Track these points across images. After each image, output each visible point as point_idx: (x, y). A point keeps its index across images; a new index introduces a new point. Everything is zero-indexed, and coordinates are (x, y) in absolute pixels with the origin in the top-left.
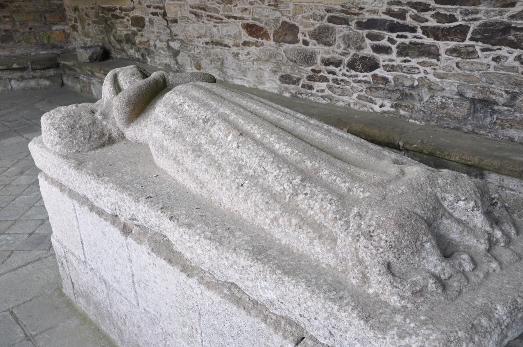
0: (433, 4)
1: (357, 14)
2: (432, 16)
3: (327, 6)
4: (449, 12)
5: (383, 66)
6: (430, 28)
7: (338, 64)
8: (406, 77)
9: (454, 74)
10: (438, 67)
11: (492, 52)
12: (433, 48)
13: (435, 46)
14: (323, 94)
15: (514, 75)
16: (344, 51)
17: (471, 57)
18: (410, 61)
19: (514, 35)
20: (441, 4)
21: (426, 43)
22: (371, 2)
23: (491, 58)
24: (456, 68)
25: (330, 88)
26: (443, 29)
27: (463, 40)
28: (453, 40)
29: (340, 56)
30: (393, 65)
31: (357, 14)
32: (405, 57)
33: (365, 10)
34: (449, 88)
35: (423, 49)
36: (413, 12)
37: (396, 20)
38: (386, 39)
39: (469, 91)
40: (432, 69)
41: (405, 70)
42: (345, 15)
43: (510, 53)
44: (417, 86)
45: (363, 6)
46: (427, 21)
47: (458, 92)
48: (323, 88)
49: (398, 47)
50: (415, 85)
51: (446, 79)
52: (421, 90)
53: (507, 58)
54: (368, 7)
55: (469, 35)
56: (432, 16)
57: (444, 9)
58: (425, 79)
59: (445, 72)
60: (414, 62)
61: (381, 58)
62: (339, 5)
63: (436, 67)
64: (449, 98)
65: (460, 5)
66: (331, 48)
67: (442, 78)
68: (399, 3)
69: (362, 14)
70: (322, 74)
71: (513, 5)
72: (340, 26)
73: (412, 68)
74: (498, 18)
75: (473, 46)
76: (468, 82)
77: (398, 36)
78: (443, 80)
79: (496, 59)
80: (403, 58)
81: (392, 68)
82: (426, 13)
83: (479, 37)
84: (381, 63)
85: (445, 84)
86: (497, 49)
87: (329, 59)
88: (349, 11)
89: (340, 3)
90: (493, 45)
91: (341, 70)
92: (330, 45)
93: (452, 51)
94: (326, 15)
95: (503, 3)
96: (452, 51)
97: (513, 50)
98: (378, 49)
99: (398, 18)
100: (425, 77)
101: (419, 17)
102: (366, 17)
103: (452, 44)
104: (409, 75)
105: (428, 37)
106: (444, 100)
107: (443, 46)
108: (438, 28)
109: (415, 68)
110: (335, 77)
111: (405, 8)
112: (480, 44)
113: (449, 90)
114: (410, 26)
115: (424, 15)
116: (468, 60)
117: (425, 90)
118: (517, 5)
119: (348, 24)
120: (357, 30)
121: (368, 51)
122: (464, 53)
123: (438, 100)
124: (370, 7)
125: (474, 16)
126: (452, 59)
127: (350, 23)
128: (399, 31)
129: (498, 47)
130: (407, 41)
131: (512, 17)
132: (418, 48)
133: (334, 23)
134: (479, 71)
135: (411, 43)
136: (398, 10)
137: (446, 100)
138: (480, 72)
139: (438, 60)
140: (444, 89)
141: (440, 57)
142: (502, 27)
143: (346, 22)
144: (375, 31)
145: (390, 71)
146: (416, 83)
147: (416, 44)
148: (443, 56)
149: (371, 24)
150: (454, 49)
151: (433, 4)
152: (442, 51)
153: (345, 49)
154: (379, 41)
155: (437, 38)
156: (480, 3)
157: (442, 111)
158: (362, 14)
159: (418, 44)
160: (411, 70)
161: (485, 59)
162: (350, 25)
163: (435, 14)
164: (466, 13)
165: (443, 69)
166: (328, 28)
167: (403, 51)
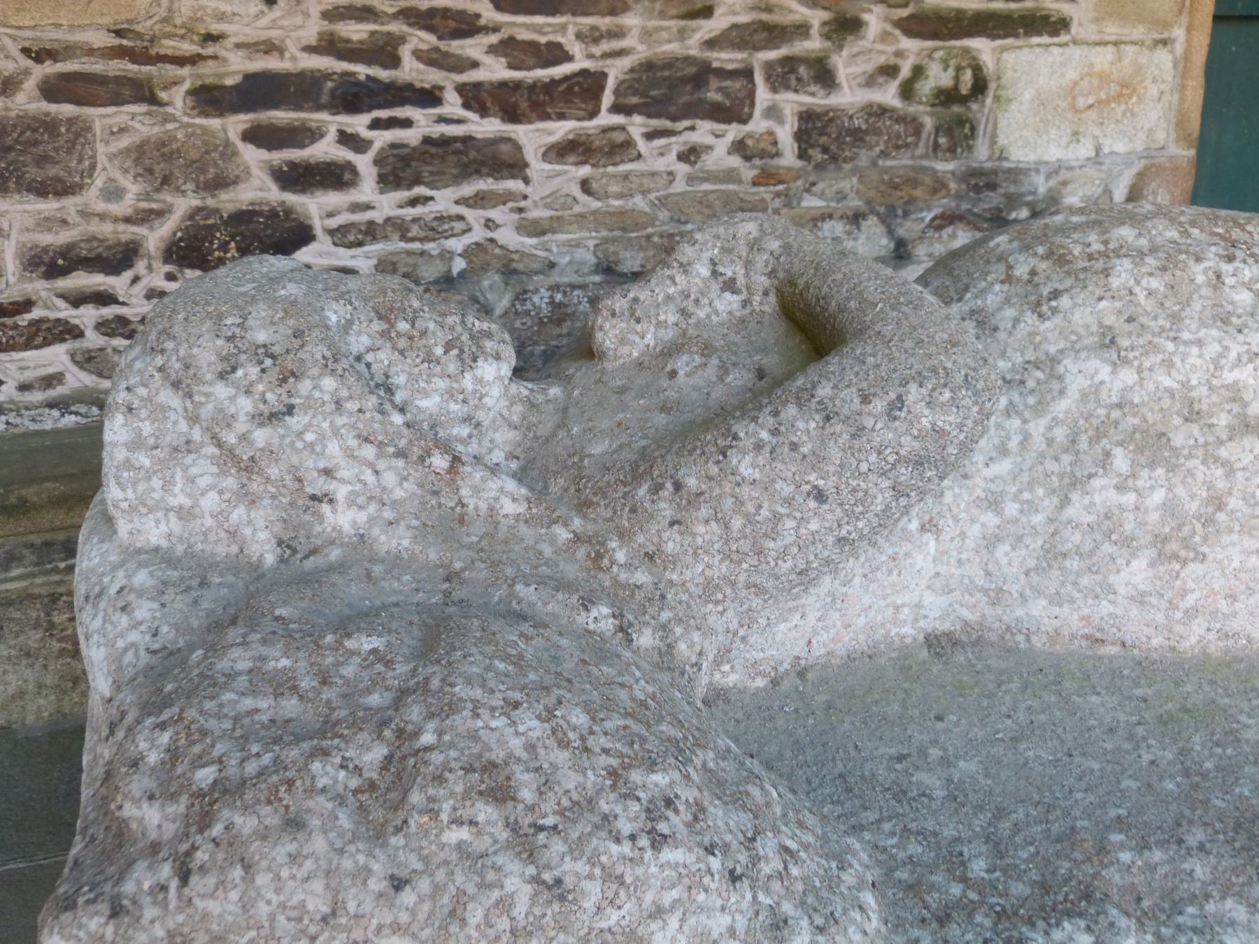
0: (489, 14)
1: (193, 60)
2: (492, 50)
3: (28, 34)
4: (545, 34)
5: (331, 232)
6: (487, 86)
7: (121, 258)
8: (423, 253)
9: (582, 216)
10: (529, 201)
11: (673, 139)
12: (505, 148)
13: (509, 140)
14: (59, 391)
15: (736, 193)
16: (144, 205)
17: (618, 159)
18: (432, 198)
19: (720, 89)
20: (516, 12)
21: (479, 136)
22: (253, 10)
23: (674, 155)
24: (583, 198)
25: (87, 360)
26: (533, 87)
27: (593, 114)
28: (562, 117)
29: (121, 227)
30: (371, 223)
31: (193, 60)
32: (410, 187)
33: (229, 43)
34: (567, 259)
35: (473, 154)
36: (421, 39)
37: (362, 70)
38: (332, 135)
39: (628, 254)
40: (512, 210)
41: (415, 231)
42: (135, 67)
43: (717, 136)
44: (462, 274)
45: (215, 28)
46: (475, 65)
47: (597, 265)
48: (51, 370)
49: (377, 162)
50: (455, 271)
51: (554, 232)
52: (479, 282)
53: (710, 148)
54: (236, 31)
55: (607, 99)
56: (492, 50)
57: (524, 25)
58: (490, 247)
59: (553, 213)
60: (444, 200)
61: (315, 206)
62: (99, 27)
63: (522, 204)
64: (574, 287)
65: (574, 14)
66: (71, 204)
67: (543, 233)
68: (367, 13)
69: (215, 57)
70: (36, 313)
71: (707, 12)
72: (110, 110)
73: (441, 219)
74: (673, 48)
75: (622, 128)
76: (624, 230)
77: (376, 125)
78: (546, 238)
79: (690, 155)
80: (404, 195)
81: (367, 233)
82: (468, 41)
83: (635, 100)
84: (318, 226)
85: (555, 250)
86: (687, 129)
87: (70, 247)
88: (153, 52)
89: (107, 20)
90: (674, 119)
91: (136, 280)
92: (63, 189)
93: (562, 151)
94: (27, 72)
95: (685, 9)
96: (562, 151)
97: (723, 126)
98: (299, 177)
99: (369, 63)
100: (492, 240)
101: (446, 54)
102: (233, 68)
103: (562, 129)
104: (430, 246)
105: (482, 116)
106: (559, 297)
107: (533, 137)
108: (517, 85)
109: (451, 218)
110: (109, 312)
111: (395, 27)
112: (638, 119)
113: (570, 263)
114: (418, 85)
115: (462, 47)
116: (610, 169)
117: (491, 280)
118: (718, 12)
119: (153, 100)
120: (198, 121)
121: (256, 188)
122: (600, 149)
123: (540, 300)
124: (248, 30)
125: (616, 45)
126: (566, 172)
127: (163, 95)
128: (380, 107)
129: (686, 123)
130: (411, 136)
131: (711, 44)
132: (456, 152)
133: (79, 102)
134: (644, 193)
135: (427, 140)
136: (364, 36)
137: (565, 293)
138: (652, 196)
139: (527, 181)
140: (552, 265)
141: (528, 171)
142: (693, 70)
143: (144, 93)
144: (281, 116)
145: (360, 244)
146: (459, 265)
147: (445, 142)
148: (537, 167)
149: (259, 91)
150: (571, 141)
151: (489, 14)
152: (531, 154)
153: (147, 197)
154: (301, 146)
155: (512, 115)
156: (626, 9)
157: (557, 331)
158: (215, 57)
159: (455, 139)
160: (438, 228)
161: (658, 158)
162: (160, 104)
163: (502, 42)
164: (591, 37)
165: (546, 206)
166: (50, 125)
167: (399, 170)
